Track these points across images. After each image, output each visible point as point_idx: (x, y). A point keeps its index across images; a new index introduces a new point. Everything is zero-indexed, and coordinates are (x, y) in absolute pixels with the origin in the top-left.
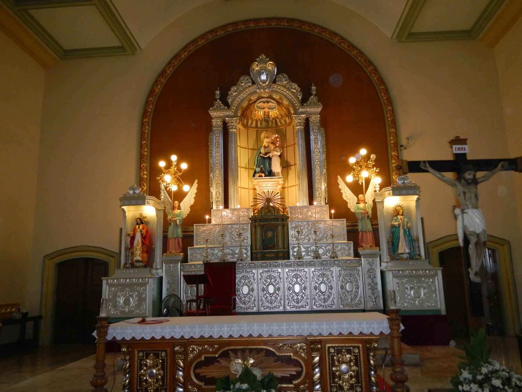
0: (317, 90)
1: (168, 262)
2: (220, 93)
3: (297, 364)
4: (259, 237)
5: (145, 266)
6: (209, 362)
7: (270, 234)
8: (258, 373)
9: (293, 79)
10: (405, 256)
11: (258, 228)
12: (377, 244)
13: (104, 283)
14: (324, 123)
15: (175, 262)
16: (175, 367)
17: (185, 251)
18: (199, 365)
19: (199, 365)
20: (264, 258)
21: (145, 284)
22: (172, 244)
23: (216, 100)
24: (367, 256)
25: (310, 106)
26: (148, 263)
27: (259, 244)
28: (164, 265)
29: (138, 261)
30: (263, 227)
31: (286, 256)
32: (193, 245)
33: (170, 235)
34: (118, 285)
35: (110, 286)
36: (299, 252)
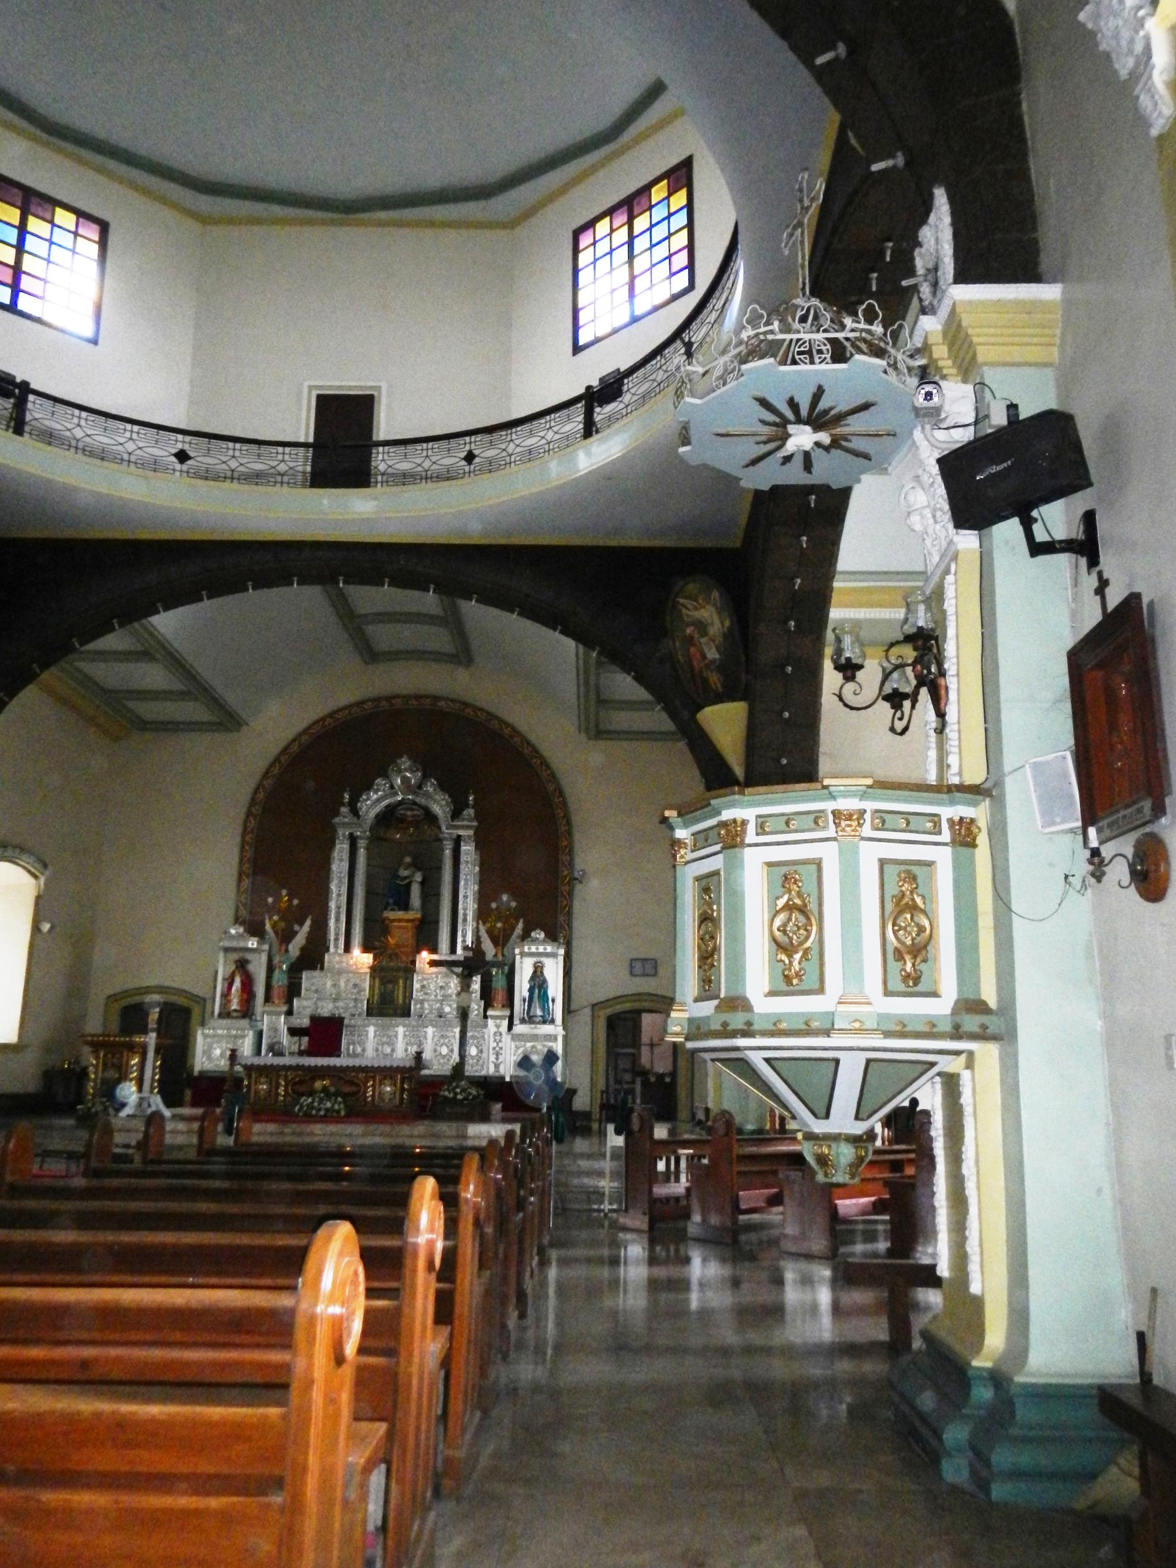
0: (475, 799)
1: (270, 1013)
2: (351, 797)
3: (357, 1085)
4: (377, 991)
5: (243, 1017)
6: (301, 1082)
7: (390, 986)
8: (332, 1089)
9: (442, 786)
10: (538, 1019)
11: (377, 981)
12: (510, 1003)
13: (199, 1032)
14: (481, 843)
15: (279, 1014)
16: (278, 1085)
17: (289, 1002)
18: (295, 1084)
19: (295, 1084)
20: (381, 1014)
21: (243, 1037)
22: (275, 992)
23: (343, 804)
24: (493, 1017)
25: (463, 820)
26: (247, 1012)
27: (376, 997)
28: (265, 1017)
29: (235, 1010)
30: (381, 980)
31: (406, 1013)
32: (299, 994)
33: (274, 983)
34: (214, 1036)
35: (205, 1036)
36: (422, 1008)
